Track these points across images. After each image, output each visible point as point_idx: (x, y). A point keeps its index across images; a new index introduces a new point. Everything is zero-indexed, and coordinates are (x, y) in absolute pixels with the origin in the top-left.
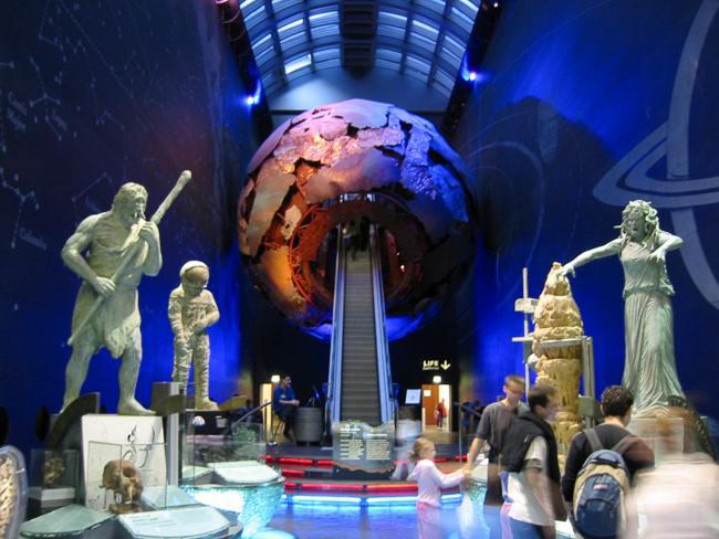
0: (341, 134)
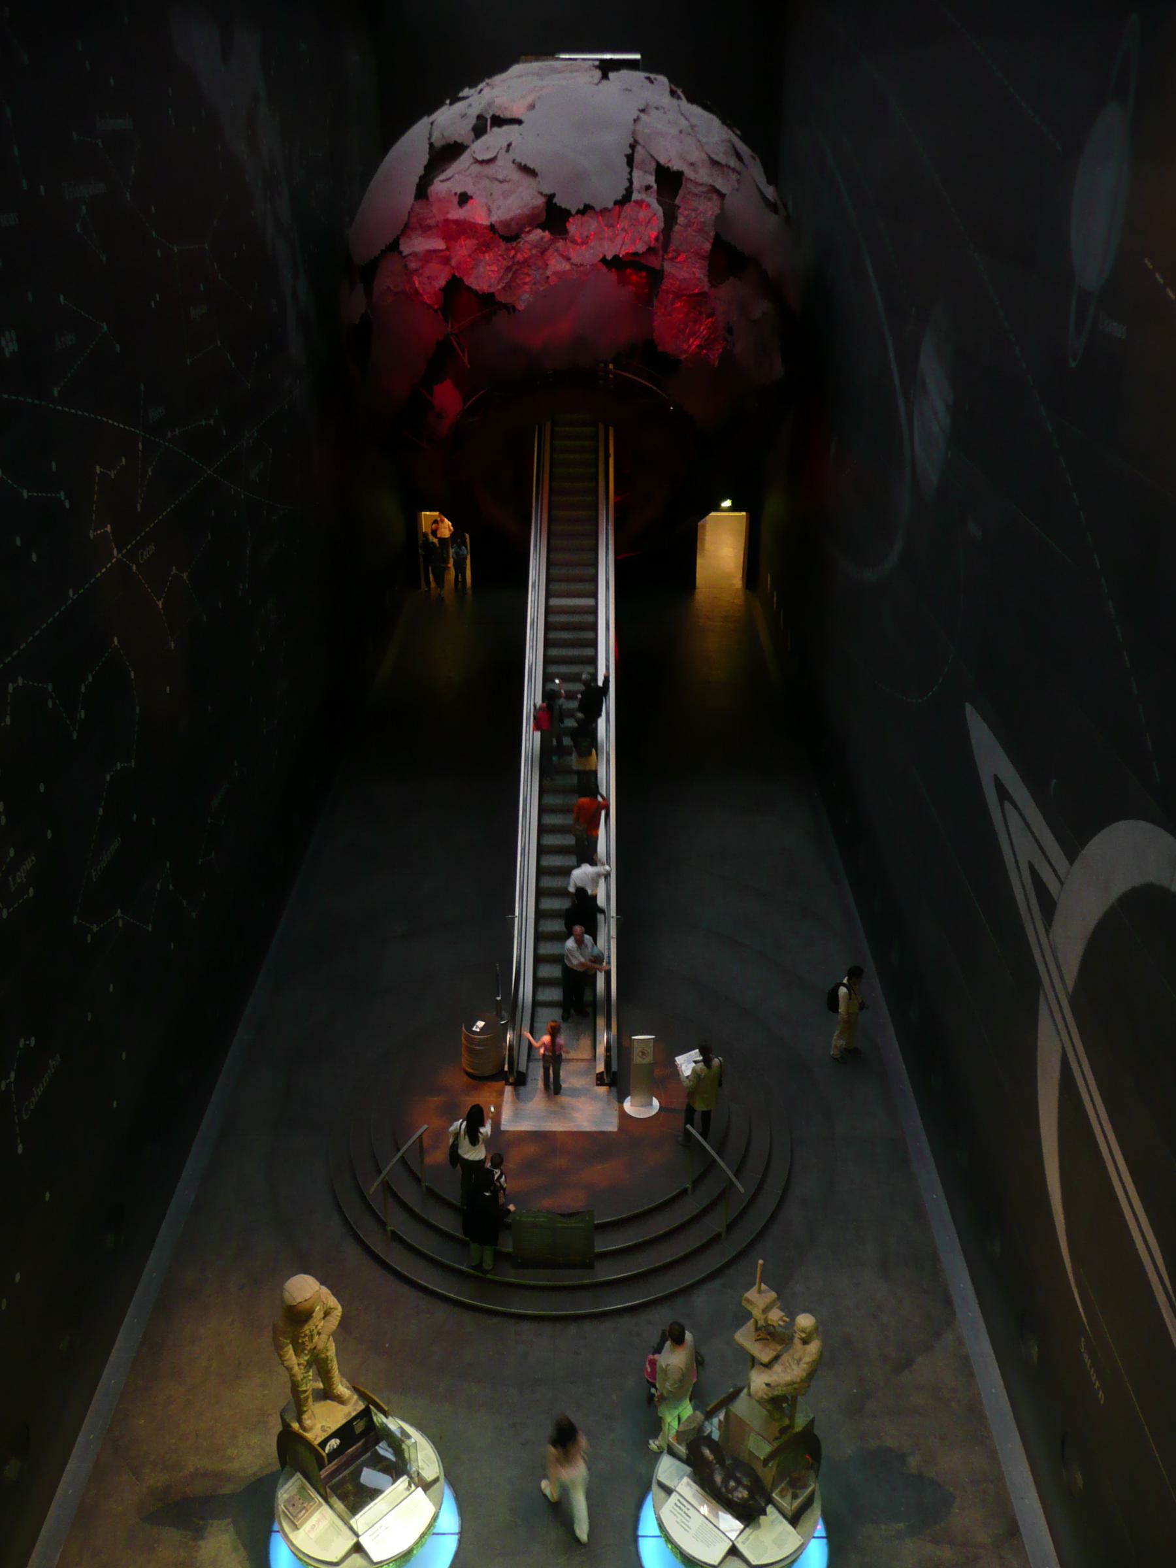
0: (531, 220)
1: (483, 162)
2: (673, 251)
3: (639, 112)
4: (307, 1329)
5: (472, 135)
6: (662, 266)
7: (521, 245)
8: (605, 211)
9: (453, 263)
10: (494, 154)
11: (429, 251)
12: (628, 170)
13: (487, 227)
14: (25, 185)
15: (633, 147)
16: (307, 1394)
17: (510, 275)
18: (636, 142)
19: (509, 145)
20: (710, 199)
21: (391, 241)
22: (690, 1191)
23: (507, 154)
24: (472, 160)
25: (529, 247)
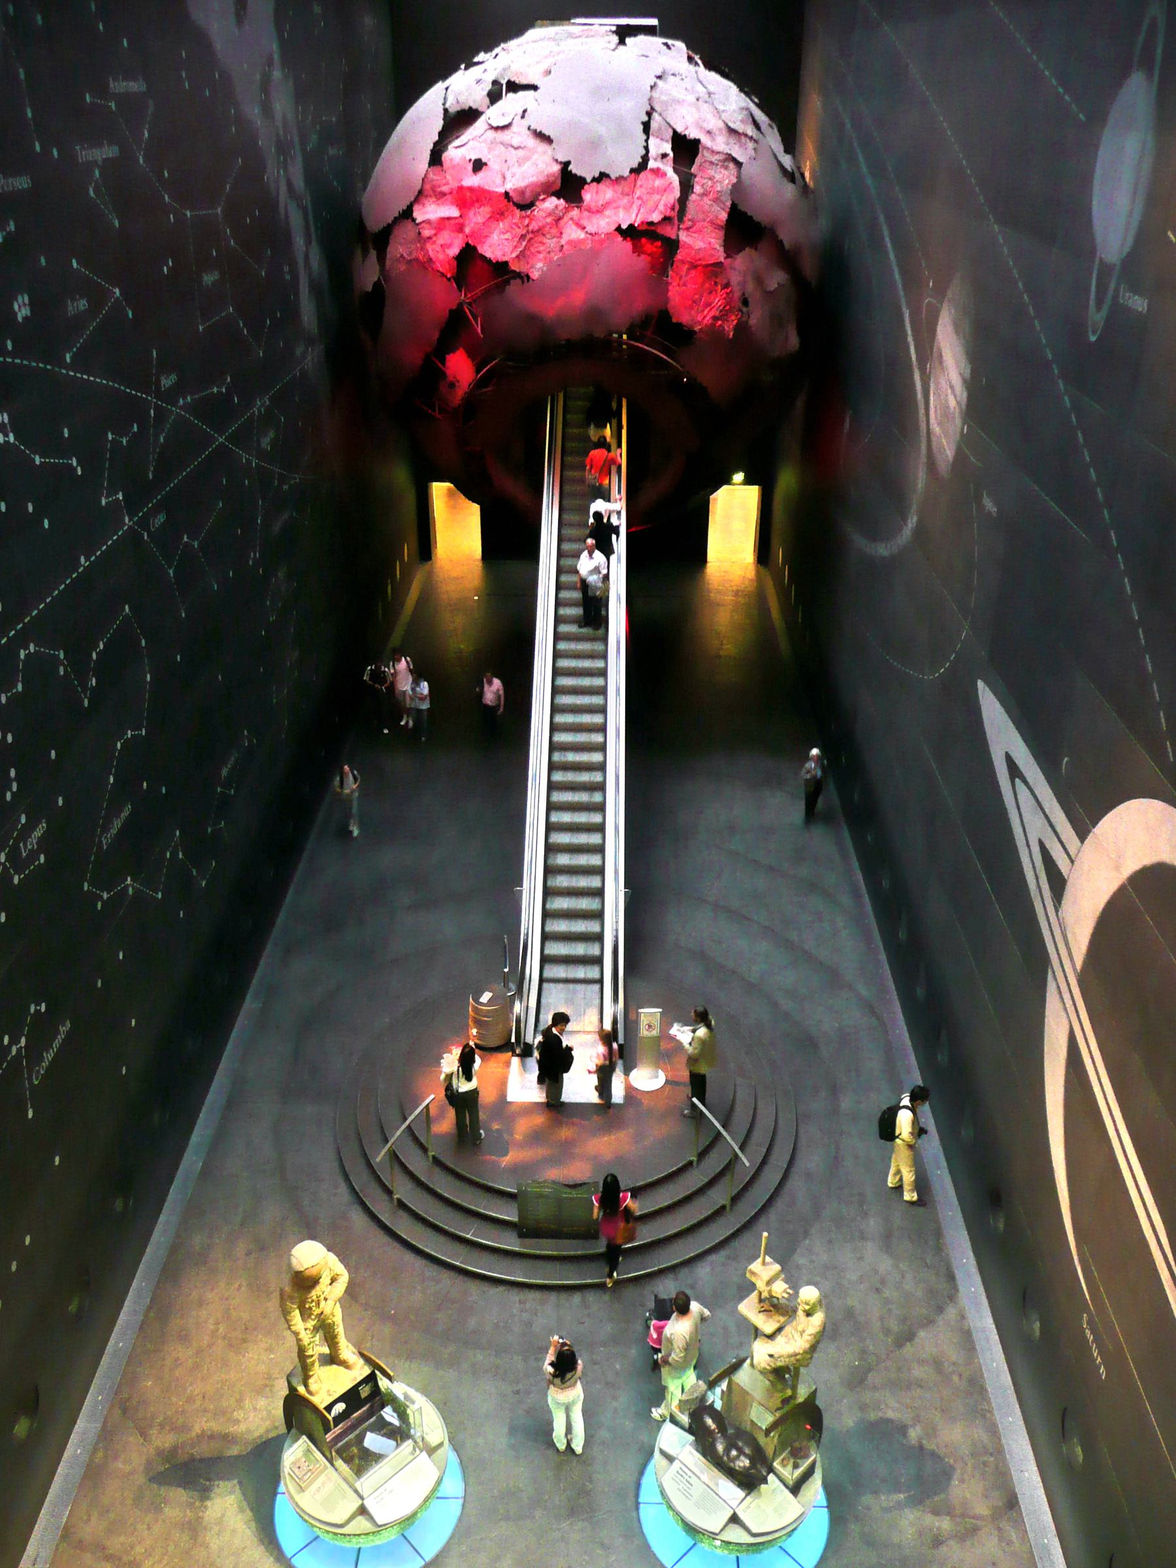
0: (547, 189)
1: (497, 128)
2: (689, 220)
3: (655, 79)
4: (314, 1294)
5: (487, 100)
6: (678, 236)
7: (535, 213)
8: (621, 178)
9: (467, 230)
10: (510, 121)
11: (443, 219)
12: (645, 137)
13: (500, 195)
14: (38, 148)
15: (649, 114)
16: (313, 1358)
17: (524, 243)
18: (652, 109)
19: (525, 111)
20: (726, 168)
21: (405, 208)
22: (695, 1164)
23: (523, 121)
24: (487, 127)
25: (544, 215)
